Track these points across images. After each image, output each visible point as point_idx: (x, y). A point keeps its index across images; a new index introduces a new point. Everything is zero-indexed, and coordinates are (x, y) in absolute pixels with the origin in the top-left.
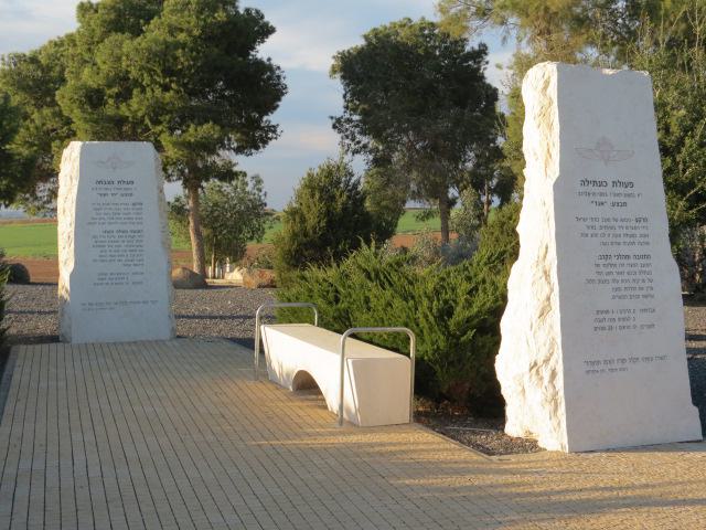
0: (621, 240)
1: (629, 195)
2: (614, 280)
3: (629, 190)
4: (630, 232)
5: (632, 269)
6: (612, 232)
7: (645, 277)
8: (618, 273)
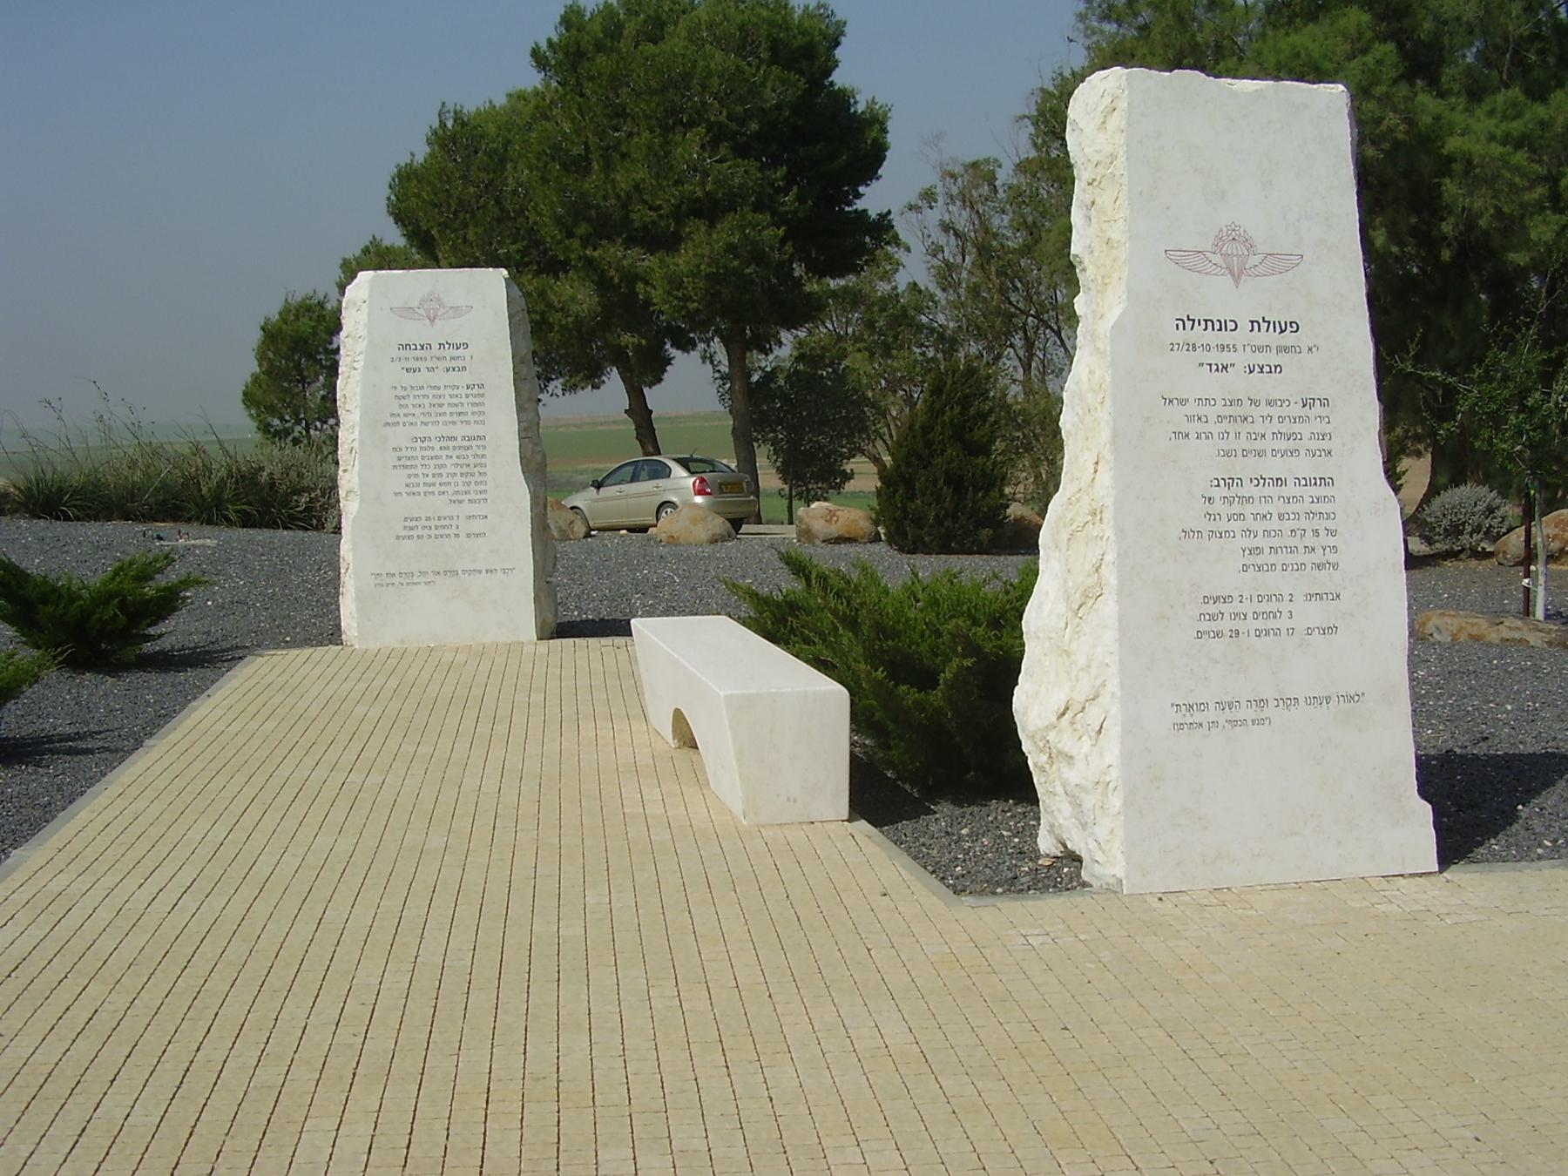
0: (1267, 444)
2: (1247, 532)
4: (1286, 428)
7: (1321, 525)
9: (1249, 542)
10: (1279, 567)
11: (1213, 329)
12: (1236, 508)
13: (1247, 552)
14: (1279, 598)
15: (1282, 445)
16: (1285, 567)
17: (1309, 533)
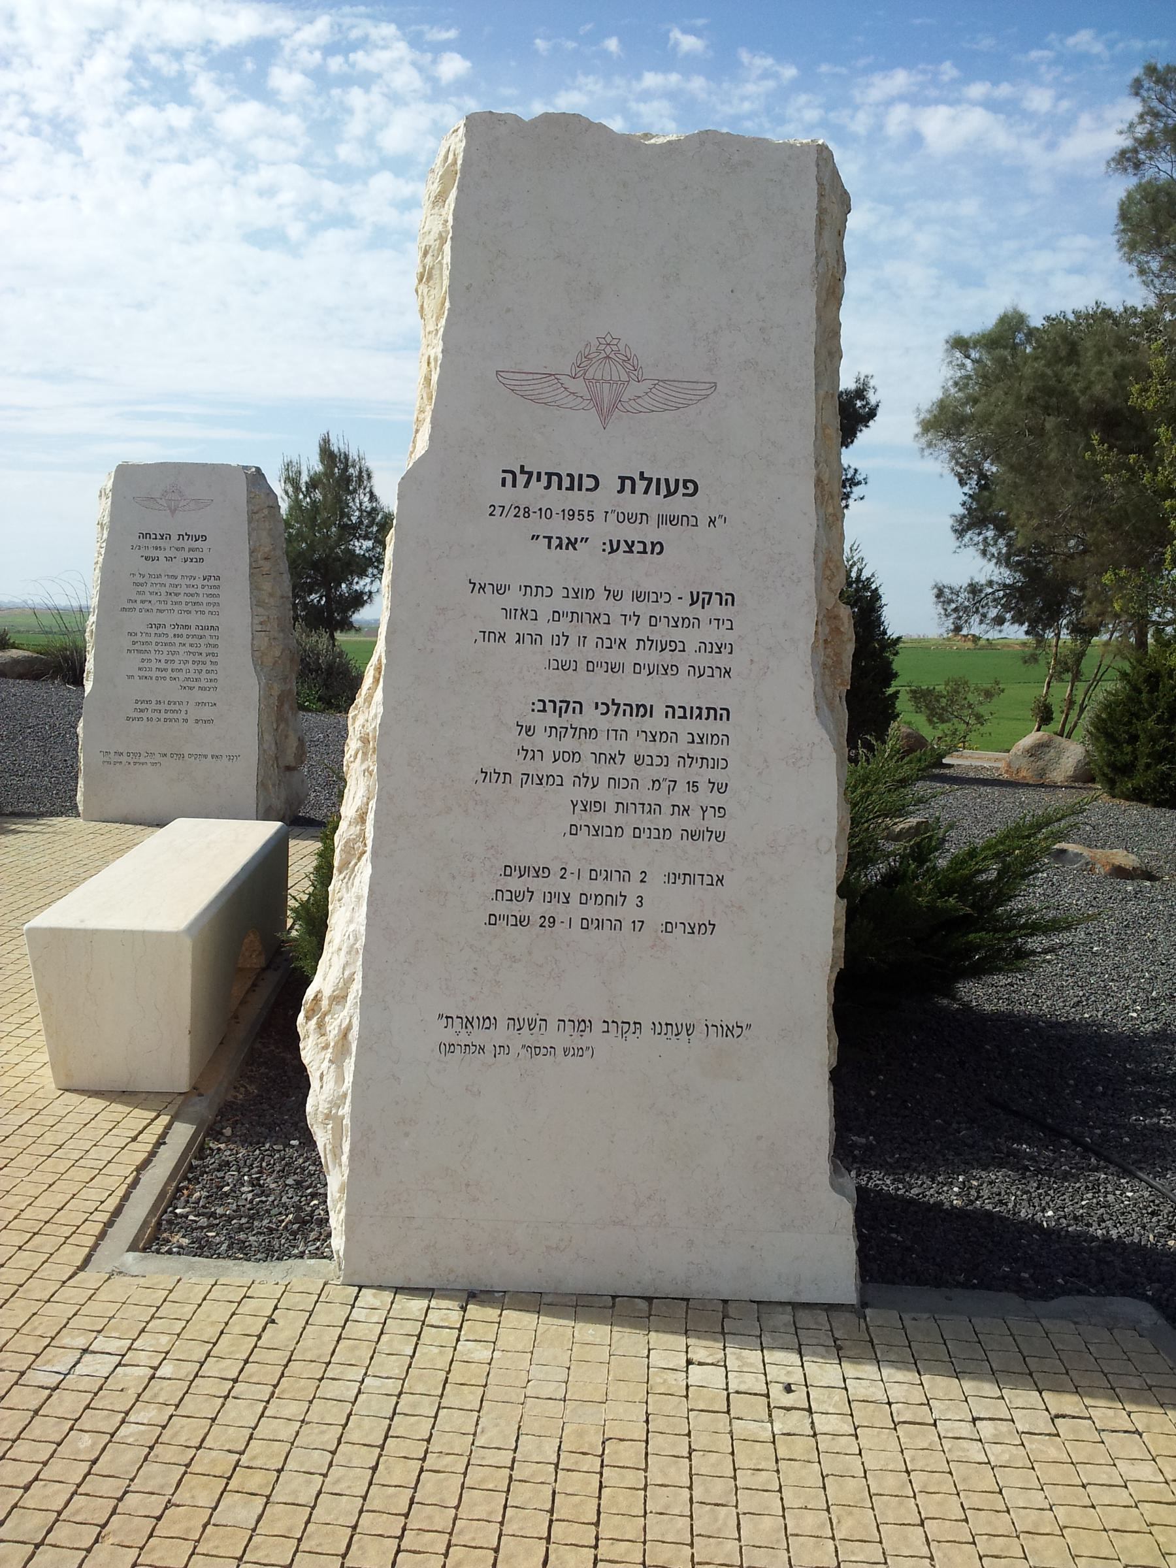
1: (672, 520)
2: (583, 779)
3: (679, 504)
4: (662, 632)
5: (654, 749)
6: (599, 630)
7: (703, 775)
8: (598, 757)
9: (583, 794)
10: (629, 832)
11: (560, 488)
12: (568, 744)
13: (580, 807)
14: (624, 875)
15: (652, 657)
16: (637, 832)
17: (682, 786)
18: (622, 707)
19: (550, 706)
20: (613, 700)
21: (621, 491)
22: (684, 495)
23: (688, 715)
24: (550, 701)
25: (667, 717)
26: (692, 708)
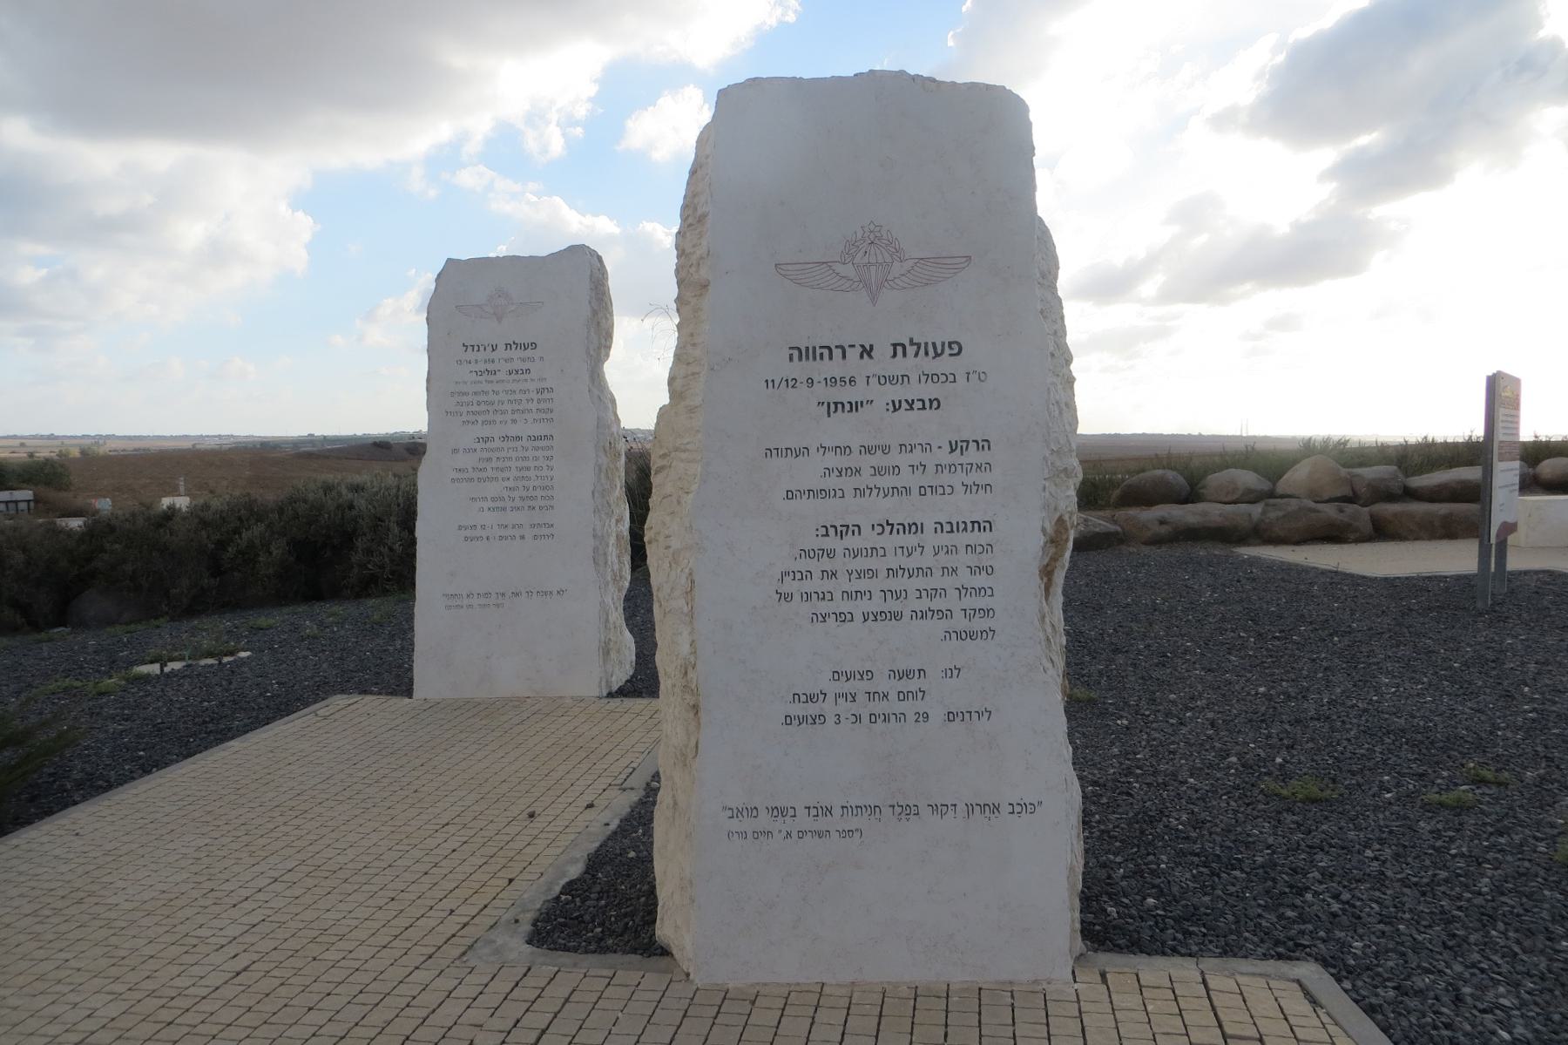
18: (896, 527)
19: (832, 531)
20: (887, 521)
21: (895, 355)
22: (951, 355)
23: (955, 529)
24: (831, 526)
25: (936, 532)
26: (958, 523)
